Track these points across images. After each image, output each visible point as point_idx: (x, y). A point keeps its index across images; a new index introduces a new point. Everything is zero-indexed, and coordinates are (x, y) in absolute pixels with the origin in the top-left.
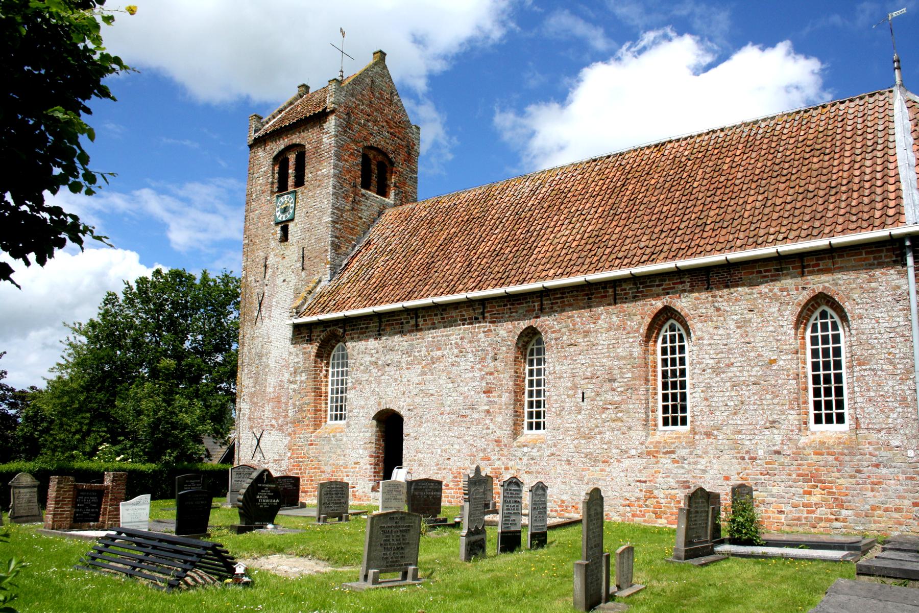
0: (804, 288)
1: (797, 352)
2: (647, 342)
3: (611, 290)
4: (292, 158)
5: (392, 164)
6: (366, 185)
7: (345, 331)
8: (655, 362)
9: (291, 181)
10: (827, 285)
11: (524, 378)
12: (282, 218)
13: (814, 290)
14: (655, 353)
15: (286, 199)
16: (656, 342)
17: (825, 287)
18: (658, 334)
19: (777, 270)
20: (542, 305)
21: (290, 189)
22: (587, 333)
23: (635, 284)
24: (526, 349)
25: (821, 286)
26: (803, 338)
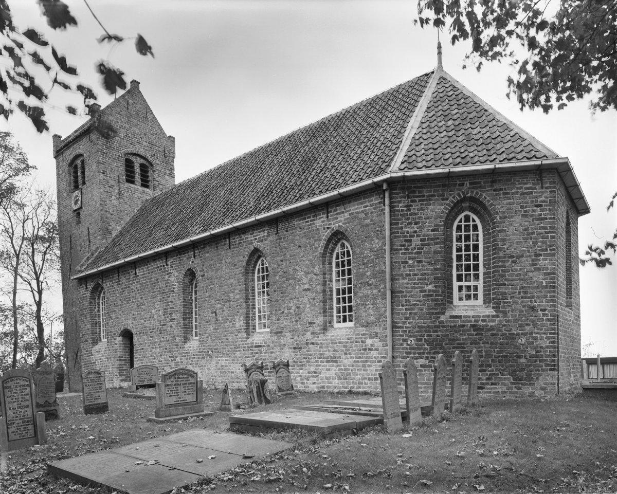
0: (328, 228)
1: (324, 274)
2: (246, 273)
3: (228, 240)
4: (79, 162)
5: (152, 165)
6: (130, 179)
7: (102, 281)
8: (254, 287)
9: (80, 181)
10: (341, 224)
11: (192, 303)
12: (75, 207)
13: (333, 229)
14: (253, 281)
15: (77, 193)
16: (253, 273)
17: (339, 226)
18: (254, 267)
19: (314, 216)
20: (194, 253)
21: (80, 187)
22: (217, 270)
23: (239, 235)
24: (192, 284)
25: (337, 225)
26: (331, 264)
